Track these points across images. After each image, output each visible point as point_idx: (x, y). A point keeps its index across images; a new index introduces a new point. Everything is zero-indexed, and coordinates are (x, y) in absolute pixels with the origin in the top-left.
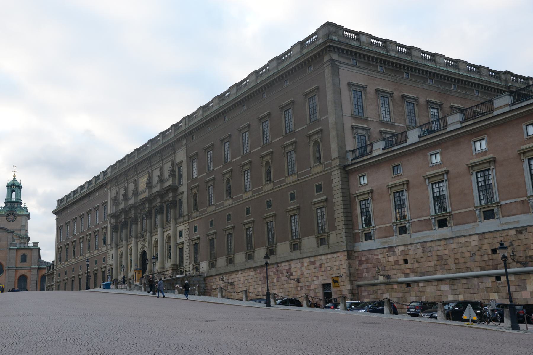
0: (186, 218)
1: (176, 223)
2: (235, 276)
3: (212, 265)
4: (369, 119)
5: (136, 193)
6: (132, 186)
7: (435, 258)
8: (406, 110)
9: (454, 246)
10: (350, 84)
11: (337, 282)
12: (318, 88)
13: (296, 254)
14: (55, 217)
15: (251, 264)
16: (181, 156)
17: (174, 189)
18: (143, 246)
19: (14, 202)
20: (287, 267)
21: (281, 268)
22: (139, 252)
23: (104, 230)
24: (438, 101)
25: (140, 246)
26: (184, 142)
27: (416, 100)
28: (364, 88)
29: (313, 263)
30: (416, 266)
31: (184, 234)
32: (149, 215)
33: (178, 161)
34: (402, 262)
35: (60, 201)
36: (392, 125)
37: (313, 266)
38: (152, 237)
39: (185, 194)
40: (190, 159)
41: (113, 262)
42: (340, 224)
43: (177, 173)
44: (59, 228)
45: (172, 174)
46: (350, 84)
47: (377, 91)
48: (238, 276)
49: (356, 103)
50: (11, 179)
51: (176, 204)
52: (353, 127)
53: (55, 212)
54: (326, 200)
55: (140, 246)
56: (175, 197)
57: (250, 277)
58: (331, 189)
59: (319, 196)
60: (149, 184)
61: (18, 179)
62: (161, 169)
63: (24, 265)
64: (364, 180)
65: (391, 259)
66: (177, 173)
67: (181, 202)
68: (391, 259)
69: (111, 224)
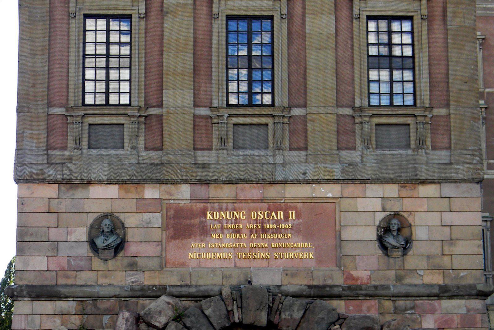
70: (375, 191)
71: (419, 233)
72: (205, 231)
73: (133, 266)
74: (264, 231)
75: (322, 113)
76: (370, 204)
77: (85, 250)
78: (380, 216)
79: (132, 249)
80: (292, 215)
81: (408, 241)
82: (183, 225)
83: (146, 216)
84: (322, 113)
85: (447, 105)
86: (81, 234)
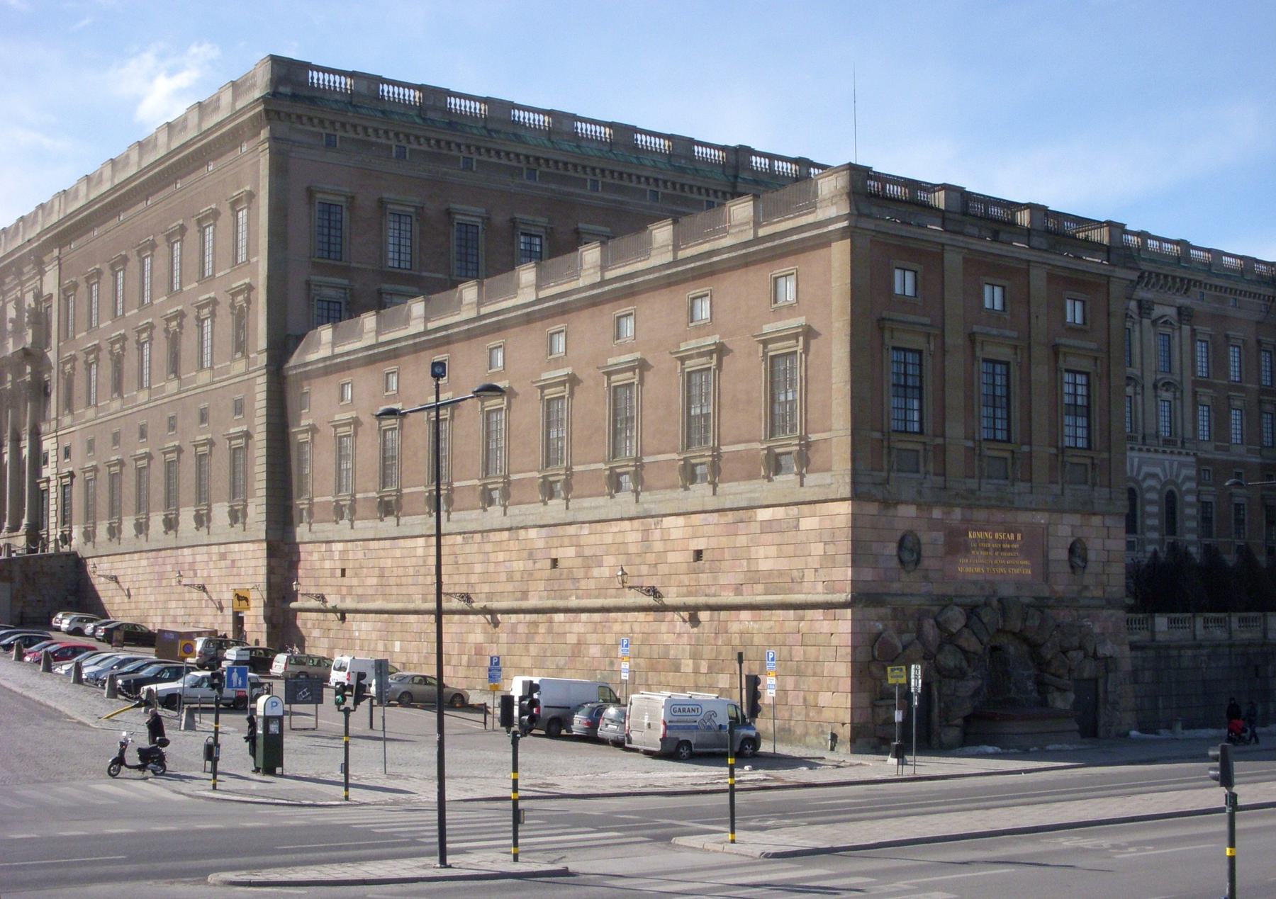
2: (119, 565)
3: (89, 536)
4: (354, 265)
7: (377, 571)
9: (398, 553)
10: (310, 192)
11: (246, 599)
13: (202, 535)
15: (142, 543)
16: (50, 284)
20: (189, 559)
21: (181, 559)
26: (56, 252)
27: (487, 220)
29: (223, 557)
30: (355, 582)
33: (46, 292)
34: (339, 573)
37: (223, 564)
40: (66, 291)
48: (124, 565)
49: (326, 231)
56: (37, 374)
57: (141, 570)
62: (19, 303)
65: (327, 564)
68: (327, 564)
71: (1092, 556)
72: (967, 549)
73: (926, 578)
74: (1002, 549)
75: (1042, 451)
76: (1065, 529)
77: (894, 563)
78: (1070, 540)
79: (926, 563)
80: (1019, 536)
81: (1085, 560)
82: (956, 544)
83: (934, 534)
84: (1042, 451)
85: (1109, 450)
86: (892, 548)
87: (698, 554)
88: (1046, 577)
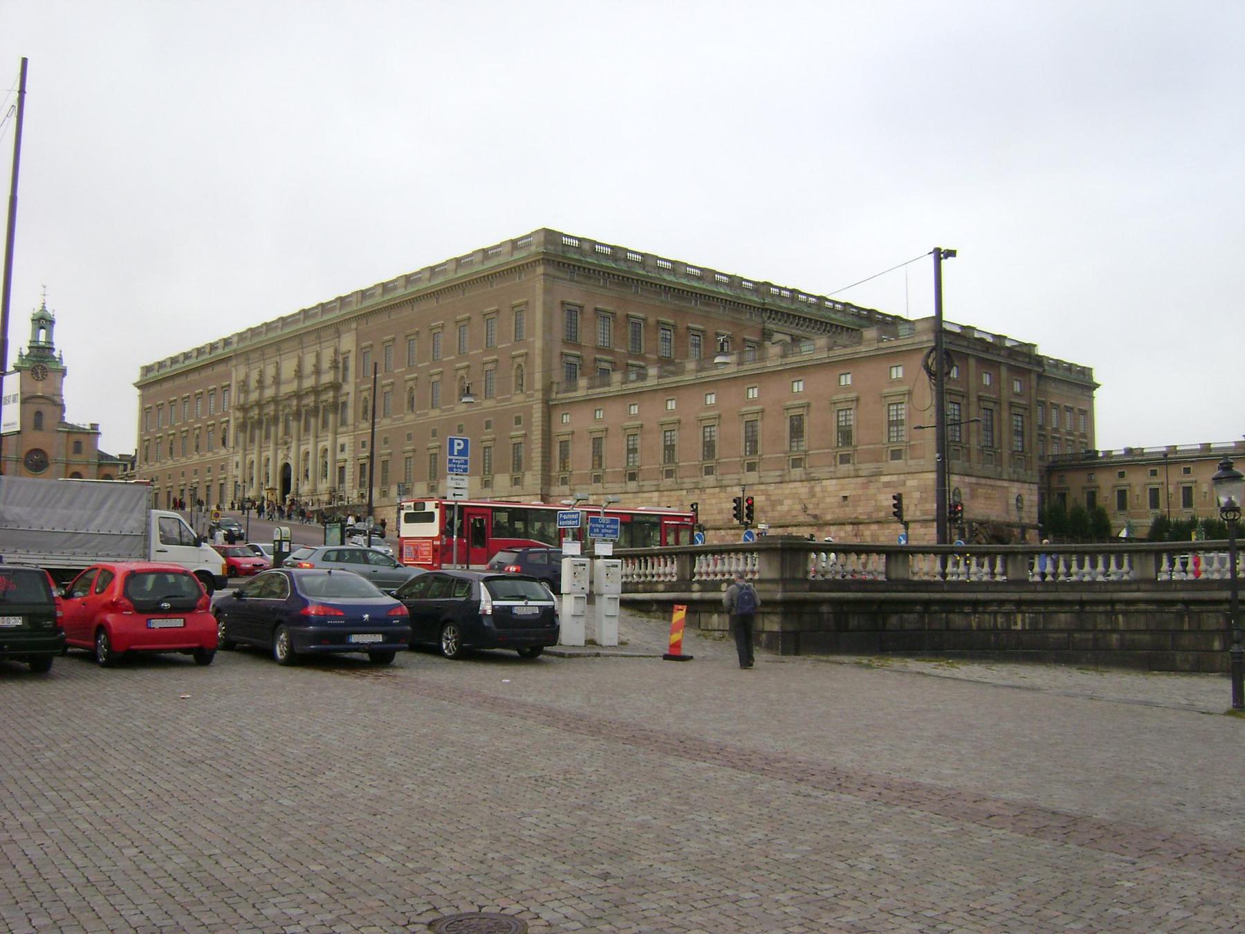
0: (351, 428)
1: (336, 433)
5: (277, 381)
6: (270, 371)
8: (630, 333)
10: (563, 303)
12: (527, 303)
14: (137, 392)
16: (348, 342)
17: (336, 387)
18: (287, 456)
19: (43, 348)
22: (280, 464)
23: (224, 425)
24: (671, 321)
25: (280, 456)
28: (581, 307)
31: (347, 449)
32: (297, 415)
35: (147, 370)
36: (610, 352)
38: (299, 446)
39: (352, 396)
41: (239, 472)
42: (537, 463)
43: (341, 365)
44: (145, 412)
45: (335, 366)
46: (563, 303)
47: (596, 310)
50: (38, 308)
51: (338, 407)
52: (562, 354)
53: (140, 386)
54: (525, 435)
55: (280, 456)
56: (336, 397)
58: (529, 424)
59: (517, 430)
60: (299, 374)
61: (49, 310)
62: (318, 356)
63: (77, 458)
64: (566, 419)
66: (341, 365)
67: (344, 404)
69: (236, 419)
70: (1017, 485)
75: (1006, 453)
84: (1006, 453)
87: (845, 498)
88: (1007, 512)
